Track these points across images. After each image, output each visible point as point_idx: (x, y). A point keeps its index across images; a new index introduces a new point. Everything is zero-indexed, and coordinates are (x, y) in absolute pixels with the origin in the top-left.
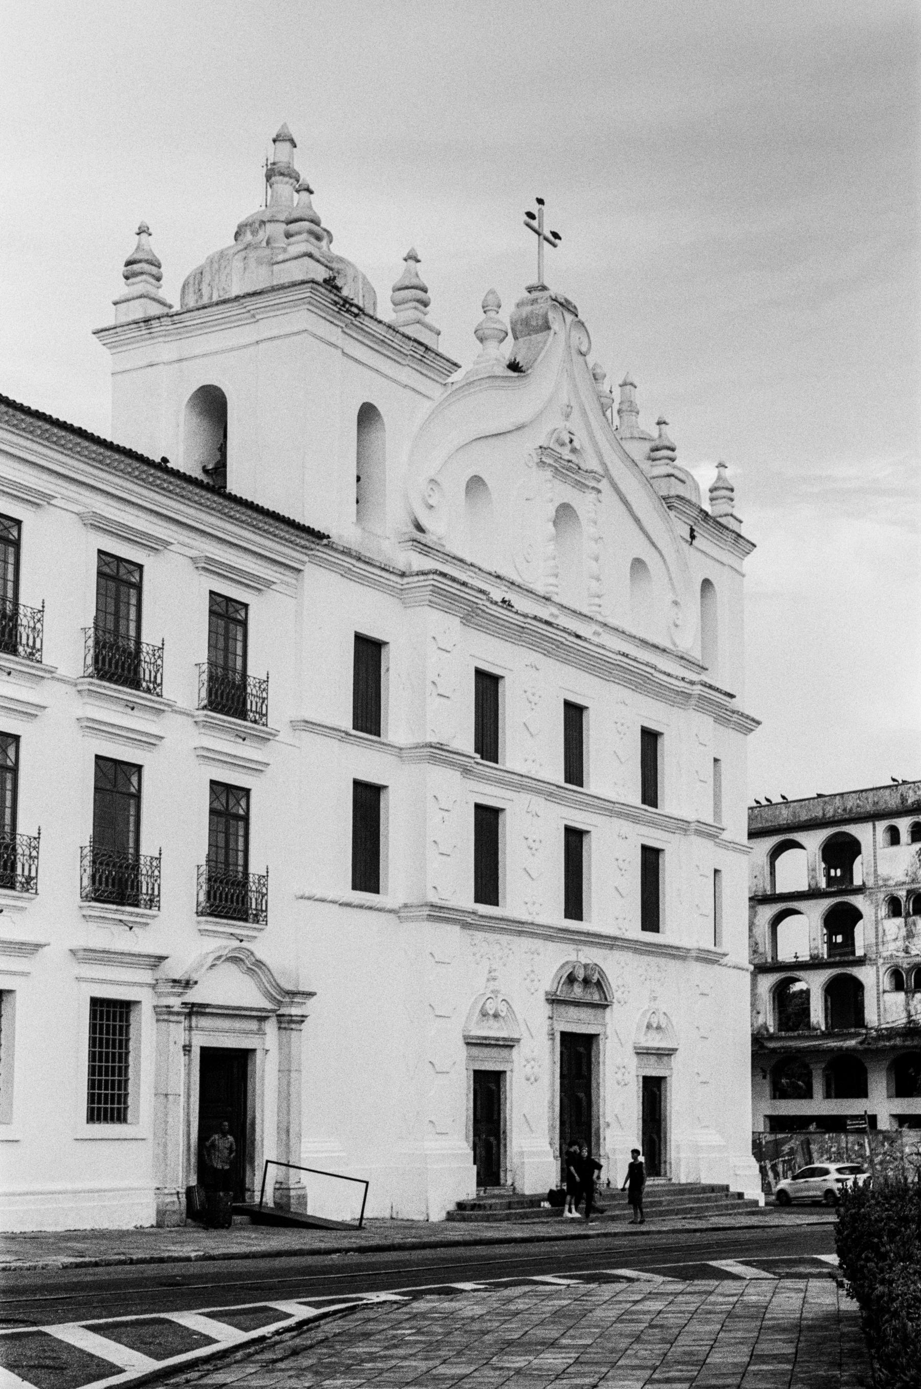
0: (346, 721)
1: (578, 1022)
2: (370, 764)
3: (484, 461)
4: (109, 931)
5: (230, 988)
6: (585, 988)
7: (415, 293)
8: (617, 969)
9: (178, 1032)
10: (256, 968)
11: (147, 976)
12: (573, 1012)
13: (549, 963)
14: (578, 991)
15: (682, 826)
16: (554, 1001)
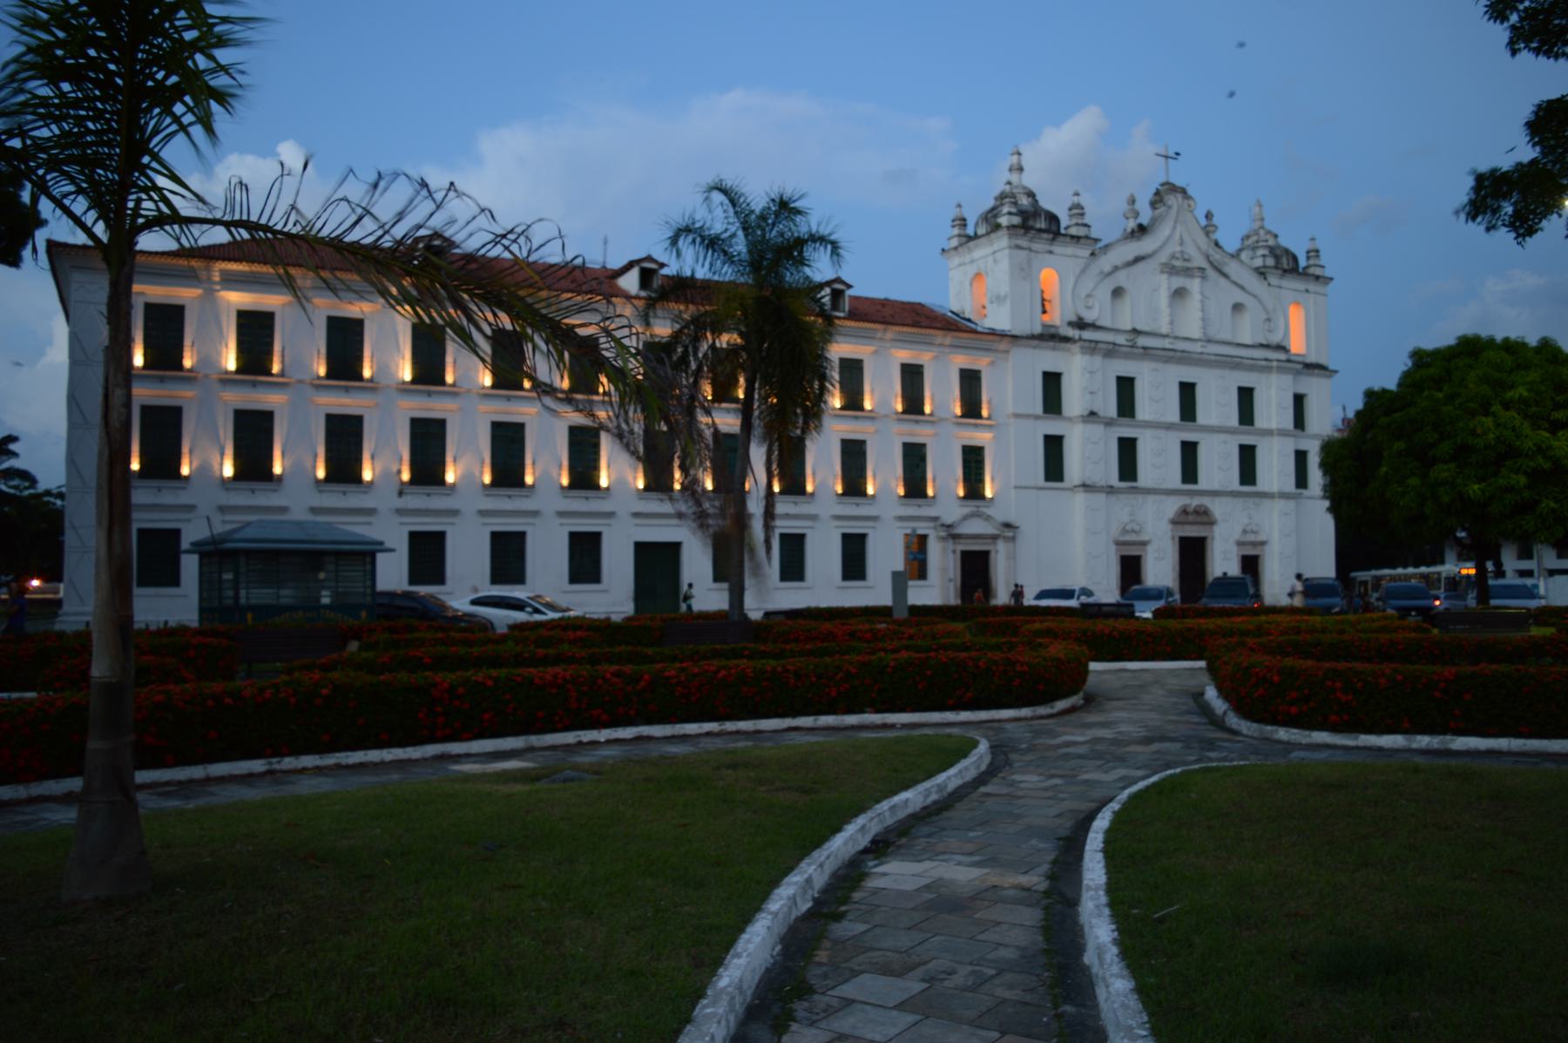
0: (1039, 409)
1: (1192, 532)
2: (1053, 427)
3: (1121, 279)
4: (912, 509)
5: (975, 527)
6: (1203, 516)
7: (1077, 209)
8: (1217, 507)
9: (950, 545)
10: (988, 518)
11: (932, 524)
12: (1188, 527)
13: (1172, 506)
14: (1191, 518)
15: (1268, 433)
16: (1174, 522)
